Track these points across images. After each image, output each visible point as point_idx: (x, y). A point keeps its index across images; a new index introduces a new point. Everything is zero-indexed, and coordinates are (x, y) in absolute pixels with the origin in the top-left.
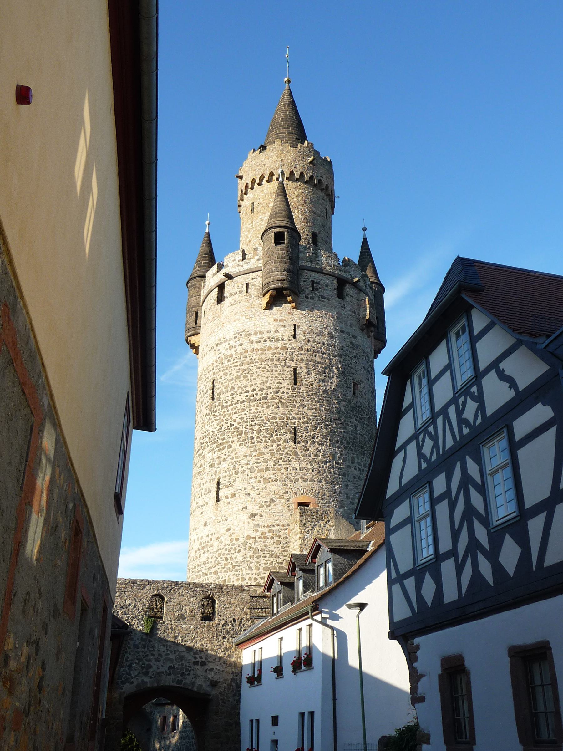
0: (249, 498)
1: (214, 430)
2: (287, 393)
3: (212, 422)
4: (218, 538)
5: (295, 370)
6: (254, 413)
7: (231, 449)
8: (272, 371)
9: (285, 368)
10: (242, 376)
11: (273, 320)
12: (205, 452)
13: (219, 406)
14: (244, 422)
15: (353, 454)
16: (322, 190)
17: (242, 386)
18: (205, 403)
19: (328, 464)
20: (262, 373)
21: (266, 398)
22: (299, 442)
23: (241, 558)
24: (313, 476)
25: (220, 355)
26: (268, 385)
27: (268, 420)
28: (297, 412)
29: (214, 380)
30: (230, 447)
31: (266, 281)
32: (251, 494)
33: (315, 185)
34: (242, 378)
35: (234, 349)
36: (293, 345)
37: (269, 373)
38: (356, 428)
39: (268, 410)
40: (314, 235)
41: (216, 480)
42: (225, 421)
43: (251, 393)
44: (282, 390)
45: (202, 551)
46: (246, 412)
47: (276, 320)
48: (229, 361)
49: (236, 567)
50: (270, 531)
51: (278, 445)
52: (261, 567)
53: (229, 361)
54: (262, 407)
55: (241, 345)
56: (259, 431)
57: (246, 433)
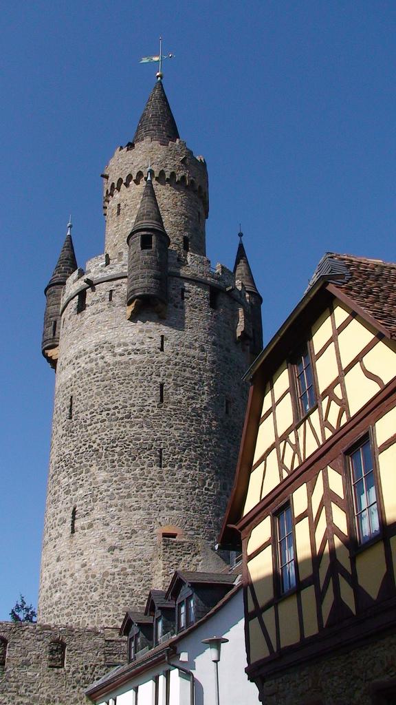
0: (109, 528)
1: (71, 452)
2: (153, 412)
4: (72, 575)
5: (162, 386)
7: (89, 474)
11: (138, 331)
12: (60, 478)
15: (225, 479)
16: (195, 191)
17: (103, 404)
18: (62, 423)
19: (197, 490)
21: (128, 417)
22: (165, 466)
23: (97, 598)
24: (180, 504)
25: (79, 369)
26: (131, 402)
28: (162, 432)
29: (72, 397)
30: (88, 471)
31: (132, 288)
32: (111, 524)
33: (187, 187)
34: (103, 394)
35: (94, 363)
36: (160, 358)
37: (133, 389)
38: (228, 451)
39: (131, 429)
40: (186, 240)
41: (72, 509)
42: (83, 443)
44: (147, 408)
45: (54, 590)
47: (141, 331)
48: (89, 375)
49: (92, 609)
50: (130, 567)
51: (142, 469)
52: (120, 609)
53: (89, 375)
54: (125, 426)
55: (103, 358)
56: (121, 454)
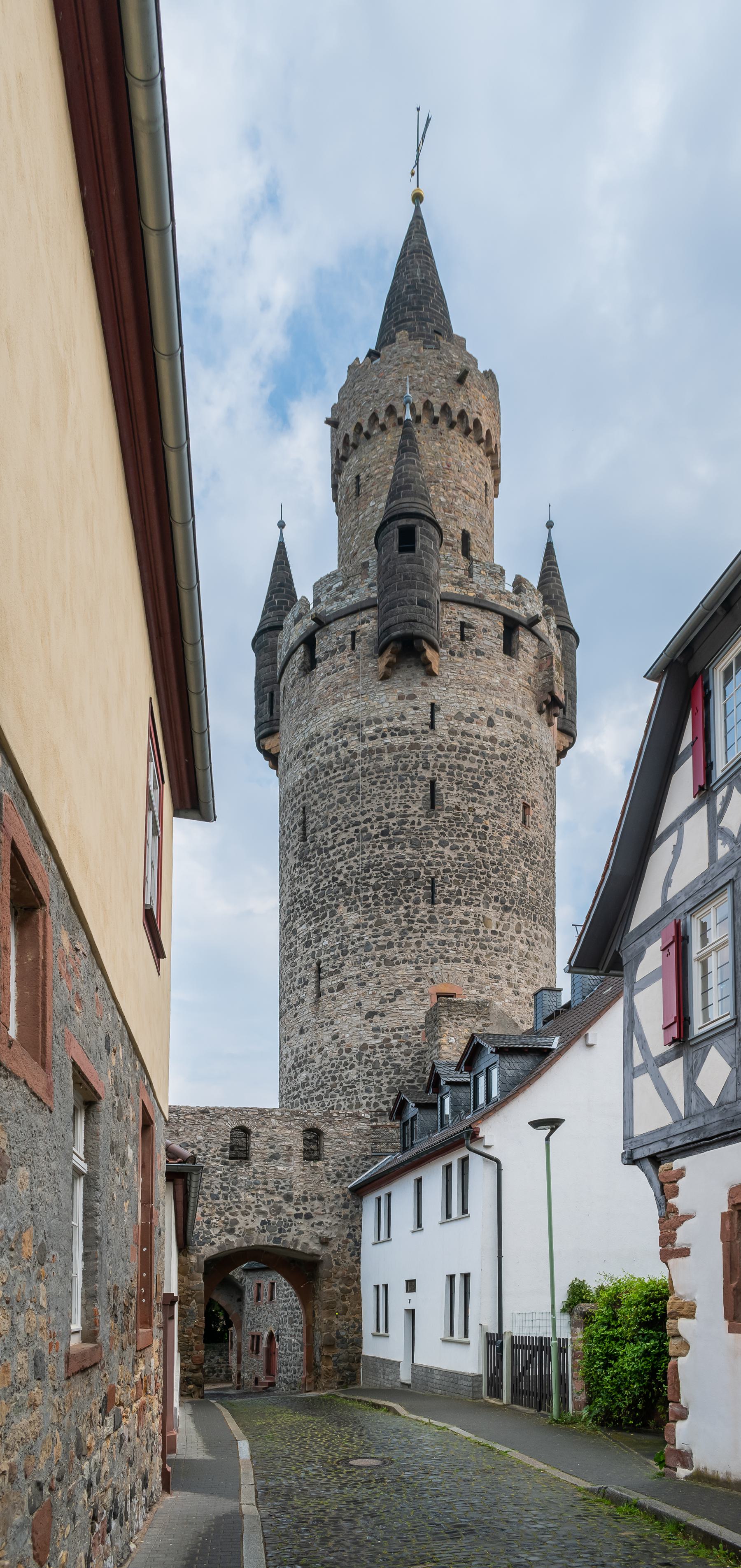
3: (305, 877)
5: (433, 783)
6: (369, 858)
7: (335, 918)
8: (395, 787)
9: (416, 782)
10: (348, 798)
13: (313, 850)
14: (353, 874)
18: (293, 848)
20: (380, 791)
21: (384, 833)
25: (313, 764)
26: (389, 810)
27: (391, 869)
30: (333, 914)
37: (390, 791)
42: (324, 874)
43: (363, 825)
44: (410, 819)
46: (356, 857)
51: (406, 908)
53: (327, 774)
54: (381, 848)
55: (345, 744)
56: (376, 888)
57: (357, 892)
